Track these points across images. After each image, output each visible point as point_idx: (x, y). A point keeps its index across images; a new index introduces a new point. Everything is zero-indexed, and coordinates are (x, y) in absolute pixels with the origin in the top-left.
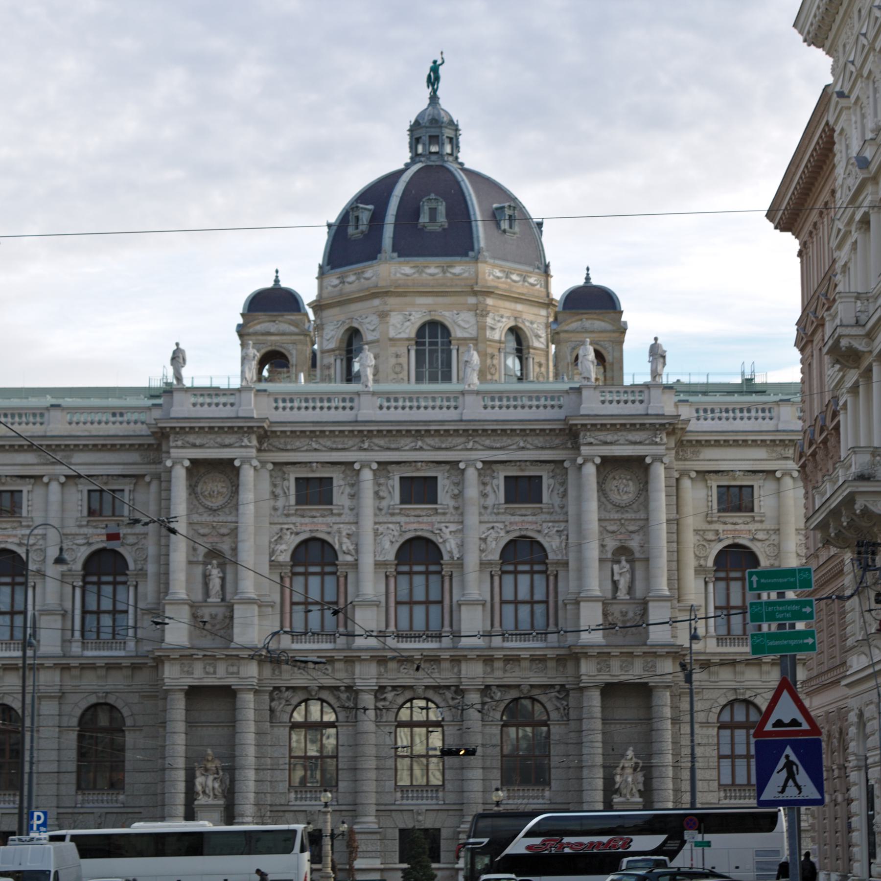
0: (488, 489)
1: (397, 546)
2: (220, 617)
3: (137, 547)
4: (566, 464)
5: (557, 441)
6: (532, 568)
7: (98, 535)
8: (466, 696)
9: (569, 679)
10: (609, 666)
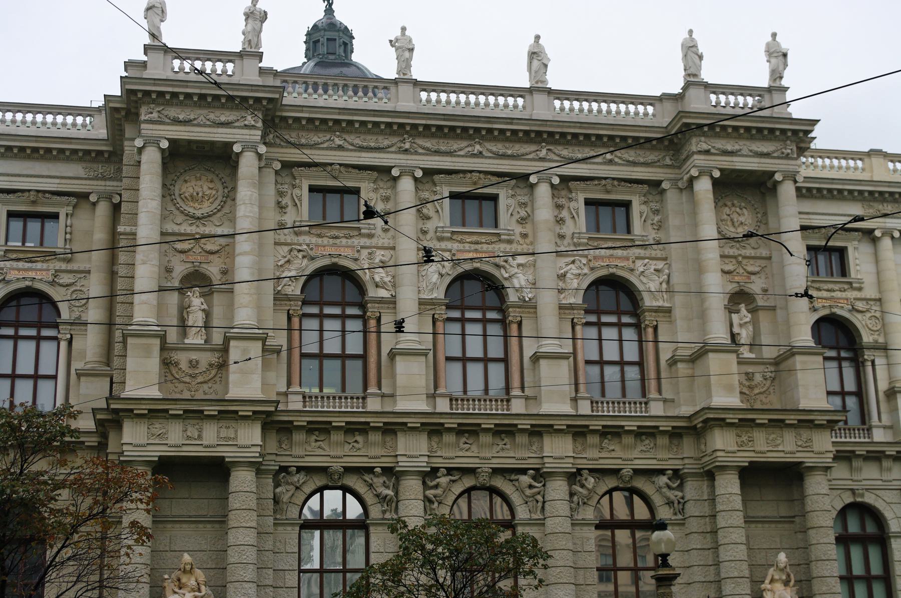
0: (565, 214)
1: (448, 280)
2: (203, 366)
3: (72, 289)
4: (664, 185)
5: (652, 157)
6: (619, 319)
7: (19, 270)
8: (549, 485)
9: (686, 461)
10: (751, 440)
